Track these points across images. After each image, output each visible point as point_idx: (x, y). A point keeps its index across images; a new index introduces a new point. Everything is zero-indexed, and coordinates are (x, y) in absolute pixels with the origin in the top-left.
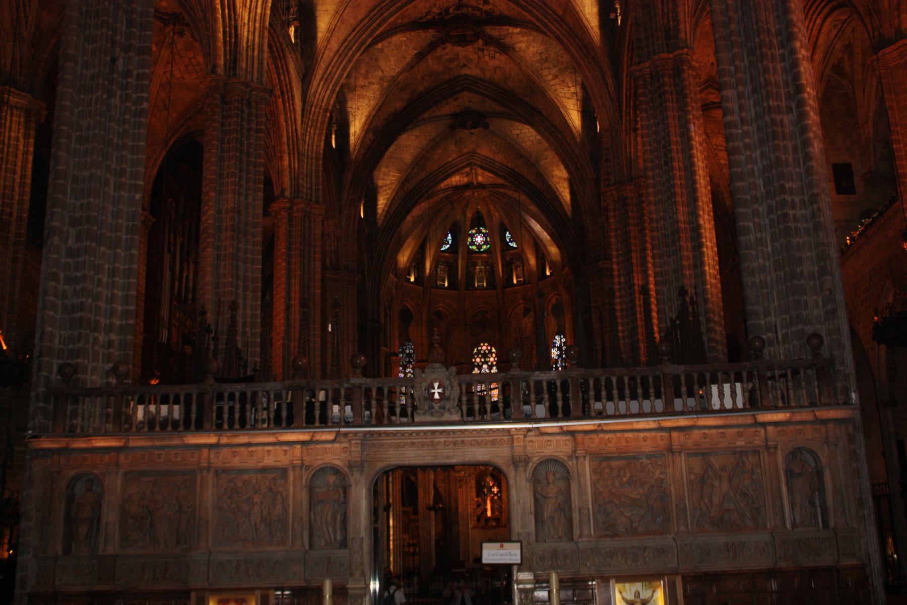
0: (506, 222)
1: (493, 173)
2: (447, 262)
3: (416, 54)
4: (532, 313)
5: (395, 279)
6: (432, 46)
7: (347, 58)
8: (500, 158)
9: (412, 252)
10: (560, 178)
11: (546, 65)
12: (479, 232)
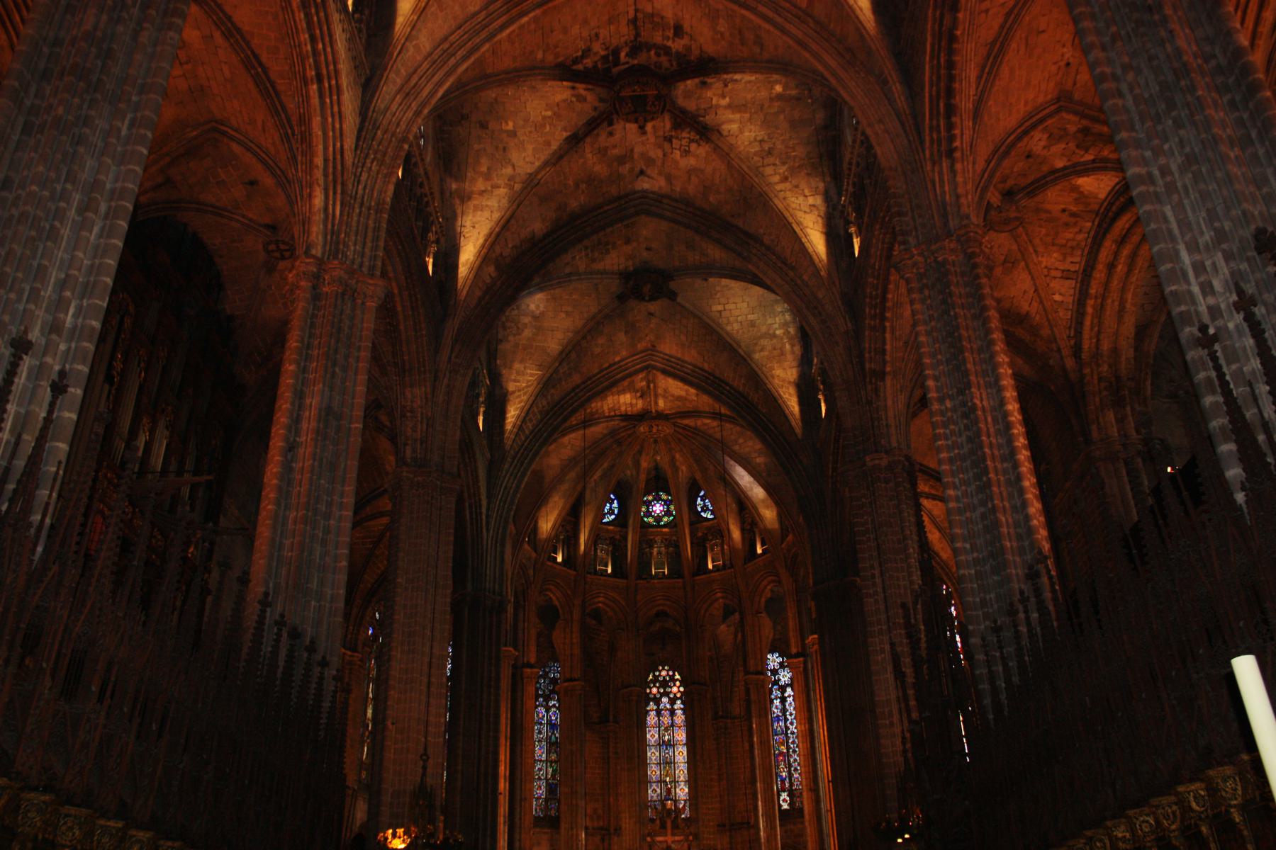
0: (698, 476)
1: (683, 380)
2: (612, 539)
3: (567, 138)
4: (737, 615)
5: (534, 555)
6: (592, 125)
7: (445, 69)
8: (691, 356)
9: (559, 515)
10: (784, 380)
11: (771, 160)
12: (658, 499)
